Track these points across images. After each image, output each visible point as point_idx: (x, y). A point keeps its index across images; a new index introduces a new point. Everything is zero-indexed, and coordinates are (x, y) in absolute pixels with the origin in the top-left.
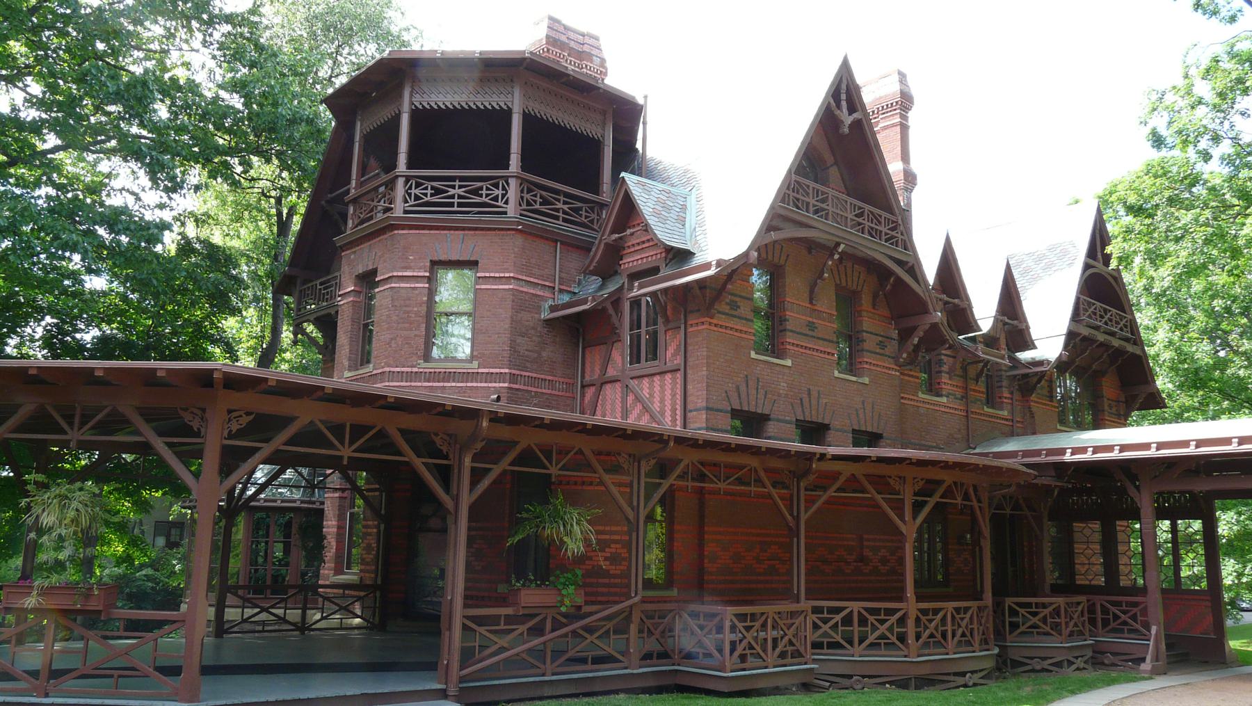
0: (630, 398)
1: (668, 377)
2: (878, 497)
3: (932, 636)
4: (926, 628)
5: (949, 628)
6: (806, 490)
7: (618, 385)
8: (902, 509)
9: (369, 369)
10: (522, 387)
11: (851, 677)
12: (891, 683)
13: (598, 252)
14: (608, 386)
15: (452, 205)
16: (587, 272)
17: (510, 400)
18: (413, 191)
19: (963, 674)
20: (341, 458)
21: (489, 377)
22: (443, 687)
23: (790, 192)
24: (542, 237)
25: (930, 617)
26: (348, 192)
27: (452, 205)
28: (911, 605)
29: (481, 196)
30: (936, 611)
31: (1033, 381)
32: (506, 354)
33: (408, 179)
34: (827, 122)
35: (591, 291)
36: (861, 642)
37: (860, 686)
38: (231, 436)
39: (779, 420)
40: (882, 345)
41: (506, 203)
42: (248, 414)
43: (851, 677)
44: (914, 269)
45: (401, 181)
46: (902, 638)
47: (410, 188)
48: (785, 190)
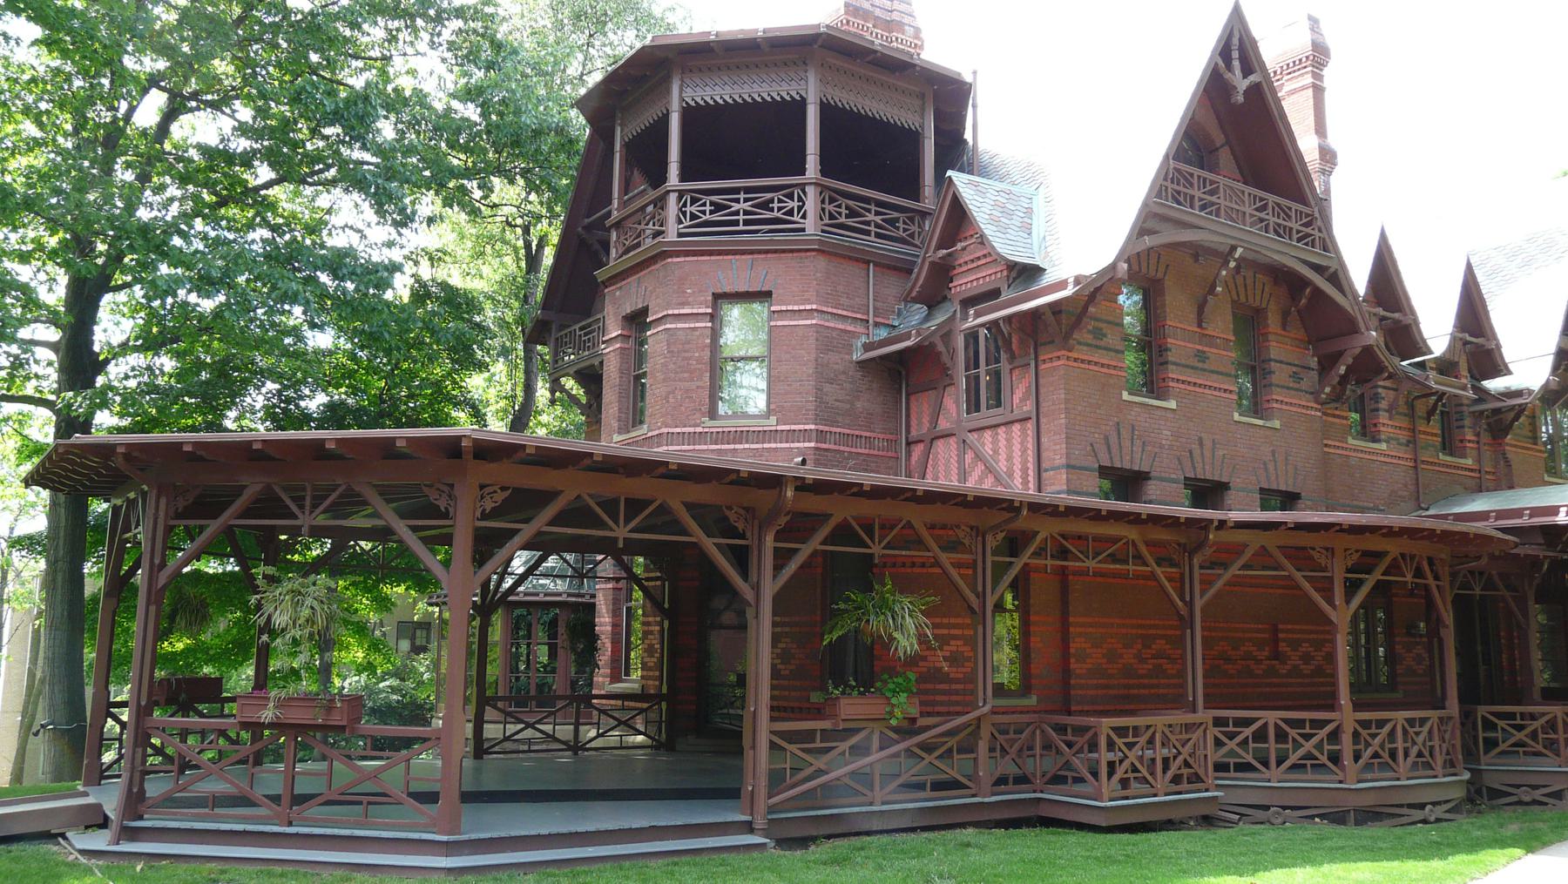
0: (969, 457)
1: (1016, 427)
2: (1298, 575)
3: (1376, 755)
4: (1368, 745)
5: (1400, 745)
6: (1201, 567)
7: (952, 440)
8: (1331, 590)
9: (643, 430)
10: (832, 446)
11: (1267, 808)
12: (1322, 816)
13: (921, 274)
14: (939, 444)
15: (736, 223)
16: (908, 299)
17: (817, 463)
18: (688, 209)
19: (1422, 806)
20: (616, 539)
21: (790, 436)
22: (748, 818)
23: (1168, 184)
24: (850, 258)
25: (1373, 731)
26: (609, 214)
27: (736, 223)
28: (1346, 715)
29: (772, 210)
30: (1381, 724)
31: (1505, 418)
33: (681, 194)
34: (1214, 88)
35: (914, 324)
36: (1279, 763)
37: (1280, 820)
38: (485, 516)
39: (1162, 479)
40: (1296, 377)
41: (804, 217)
42: (503, 489)
43: (1267, 808)
44: (1338, 277)
45: (673, 197)
46: (1335, 758)
47: (685, 205)
48: (1161, 181)
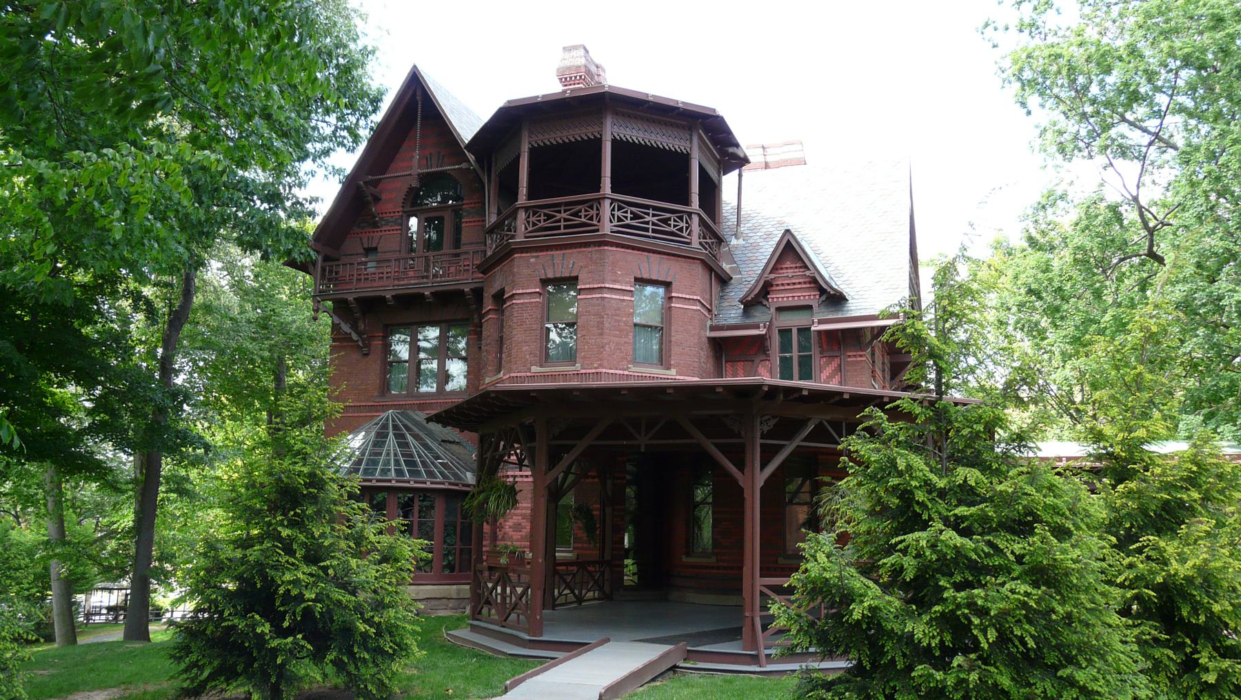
15: (647, 230)
27: (647, 230)
32: (696, 365)
45: (607, 202)
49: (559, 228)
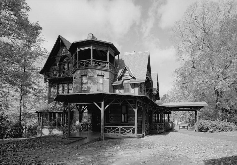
33: (93, 61)
47: (93, 62)
49: (84, 66)
